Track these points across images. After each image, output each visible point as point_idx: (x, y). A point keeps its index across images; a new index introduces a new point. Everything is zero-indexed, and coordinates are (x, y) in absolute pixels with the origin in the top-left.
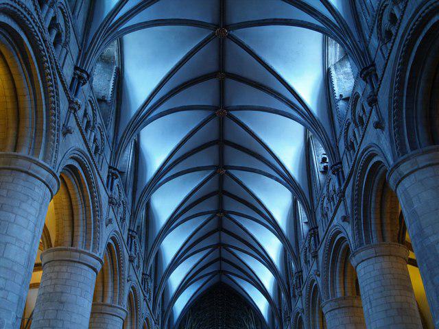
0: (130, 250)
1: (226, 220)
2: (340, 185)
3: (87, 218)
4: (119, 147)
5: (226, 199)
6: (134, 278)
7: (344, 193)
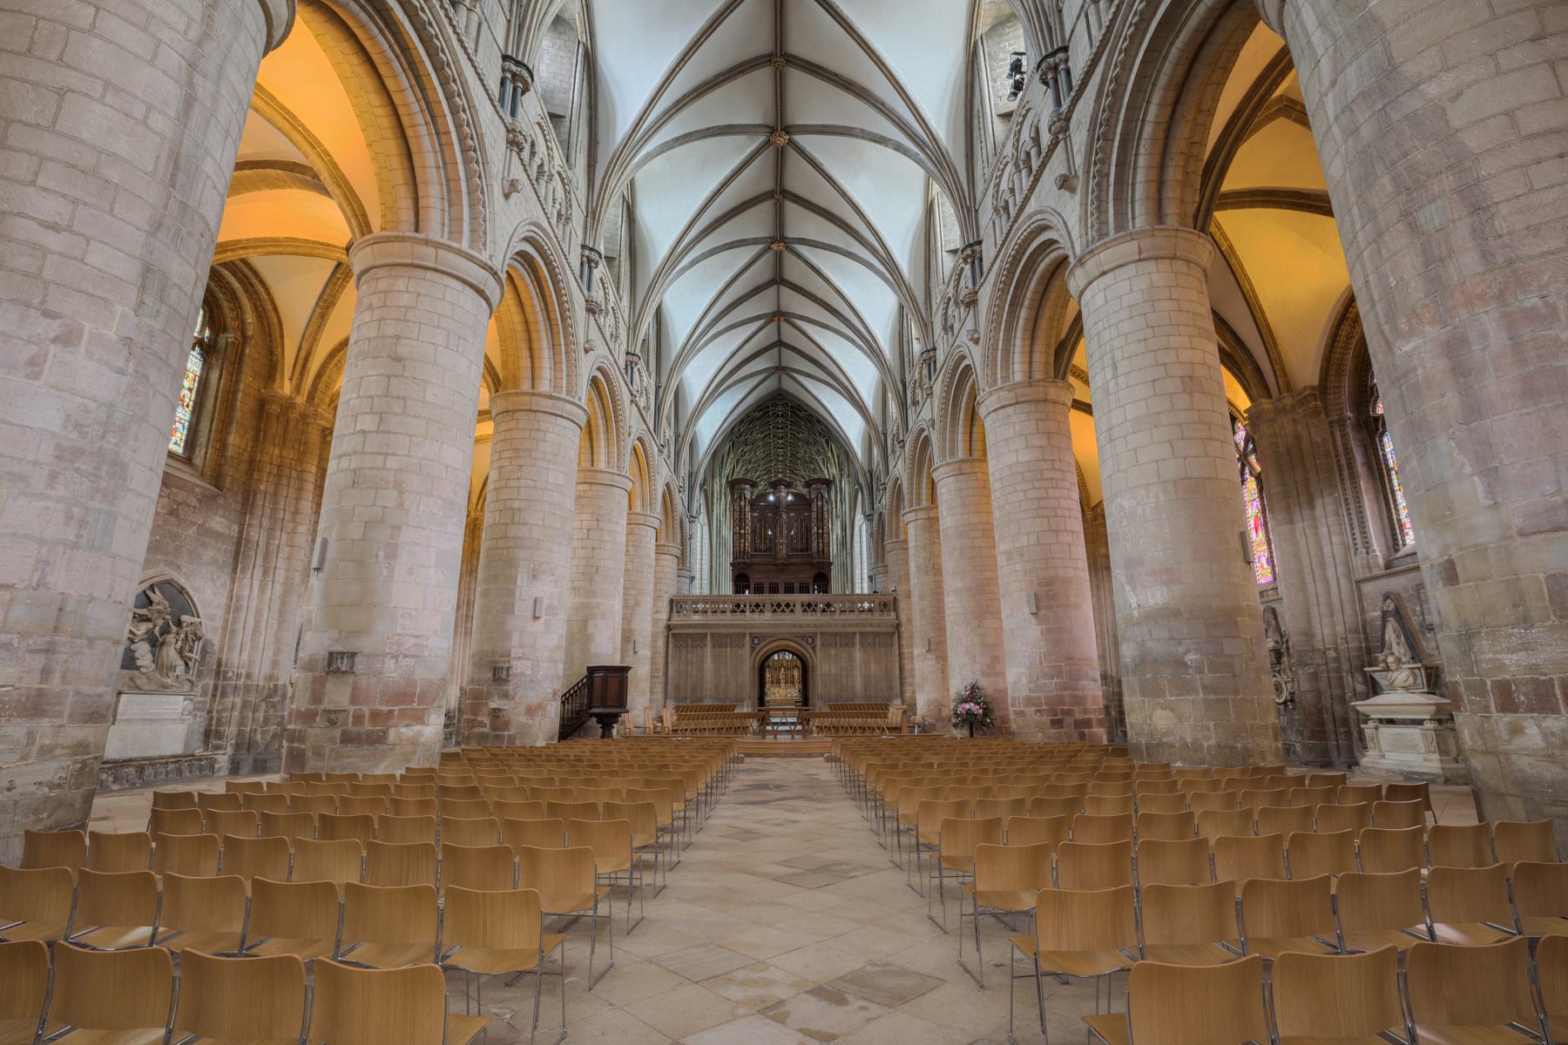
0: (589, 290)
1: (789, 259)
2: (1058, 103)
3: (447, 165)
4: (526, 11)
5: (791, 208)
6: (601, 350)
7: (1068, 120)
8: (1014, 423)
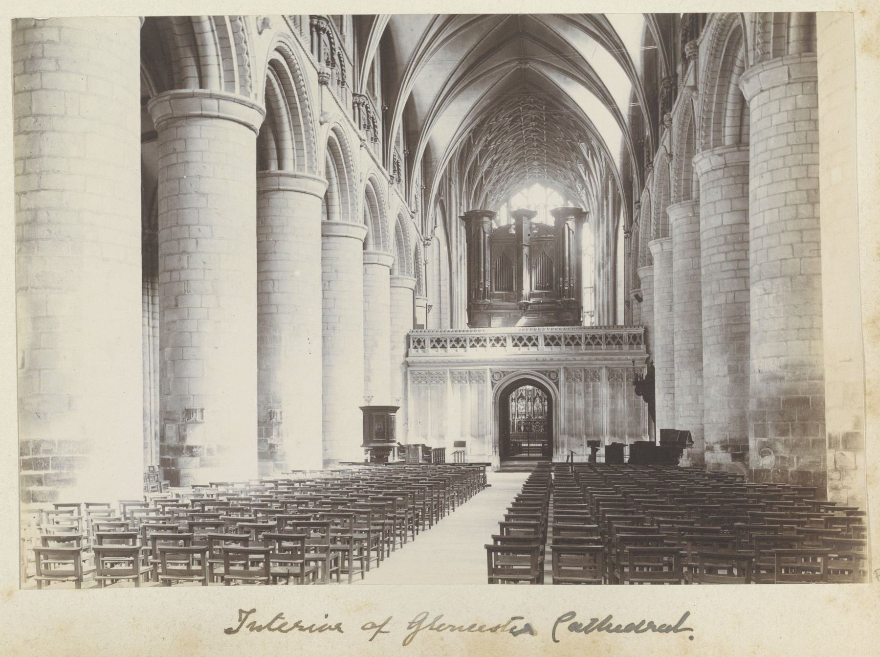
8: (722, 186)
